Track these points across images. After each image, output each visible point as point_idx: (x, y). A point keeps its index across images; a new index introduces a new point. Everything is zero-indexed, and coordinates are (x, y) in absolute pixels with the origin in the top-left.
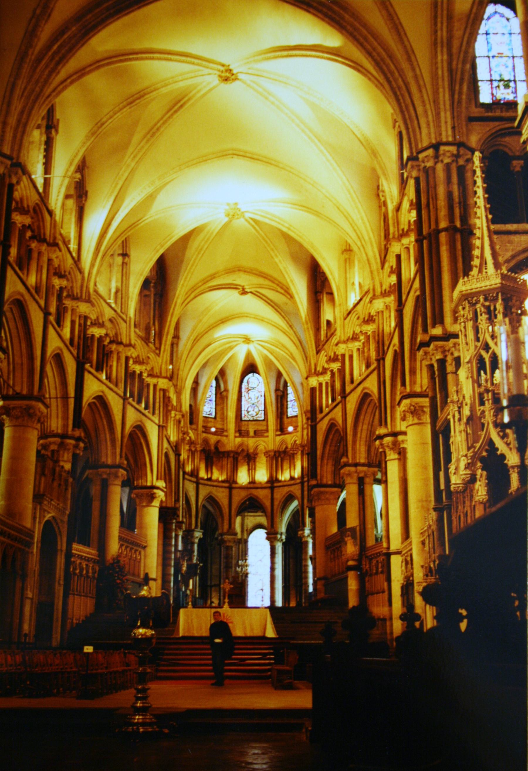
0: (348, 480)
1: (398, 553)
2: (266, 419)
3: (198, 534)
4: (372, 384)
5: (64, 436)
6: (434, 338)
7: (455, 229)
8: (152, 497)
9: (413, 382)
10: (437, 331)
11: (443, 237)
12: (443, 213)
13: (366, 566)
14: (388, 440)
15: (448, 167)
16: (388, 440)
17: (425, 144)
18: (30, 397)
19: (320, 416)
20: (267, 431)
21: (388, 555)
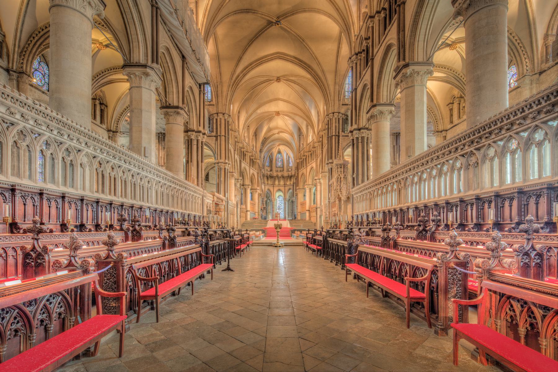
0: (307, 189)
1: (319, 208)
2: (283, 167)
3: (265, 199)
4: (314, 165)
5: (238, 179)
6: (330, 163)
7: (336, 135)
8: (256, 192)
9: (324, 169)
10: (330, 161)
11: (333, 137)
12: (334, 131)
13: (311, 210)
14: (318, 181)
15: (336, 118)
16: (318, 181)
17: (331, 112)
18: (232, 172)
19: (299, 171)
20: (283, 170)
21: (317, 208)
